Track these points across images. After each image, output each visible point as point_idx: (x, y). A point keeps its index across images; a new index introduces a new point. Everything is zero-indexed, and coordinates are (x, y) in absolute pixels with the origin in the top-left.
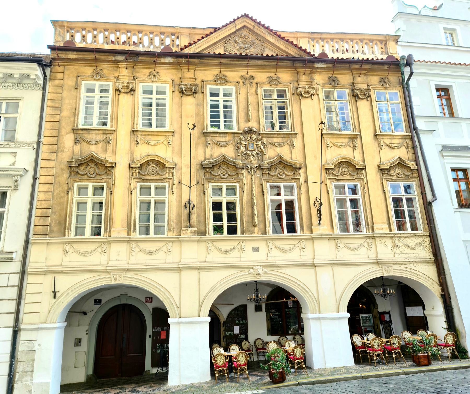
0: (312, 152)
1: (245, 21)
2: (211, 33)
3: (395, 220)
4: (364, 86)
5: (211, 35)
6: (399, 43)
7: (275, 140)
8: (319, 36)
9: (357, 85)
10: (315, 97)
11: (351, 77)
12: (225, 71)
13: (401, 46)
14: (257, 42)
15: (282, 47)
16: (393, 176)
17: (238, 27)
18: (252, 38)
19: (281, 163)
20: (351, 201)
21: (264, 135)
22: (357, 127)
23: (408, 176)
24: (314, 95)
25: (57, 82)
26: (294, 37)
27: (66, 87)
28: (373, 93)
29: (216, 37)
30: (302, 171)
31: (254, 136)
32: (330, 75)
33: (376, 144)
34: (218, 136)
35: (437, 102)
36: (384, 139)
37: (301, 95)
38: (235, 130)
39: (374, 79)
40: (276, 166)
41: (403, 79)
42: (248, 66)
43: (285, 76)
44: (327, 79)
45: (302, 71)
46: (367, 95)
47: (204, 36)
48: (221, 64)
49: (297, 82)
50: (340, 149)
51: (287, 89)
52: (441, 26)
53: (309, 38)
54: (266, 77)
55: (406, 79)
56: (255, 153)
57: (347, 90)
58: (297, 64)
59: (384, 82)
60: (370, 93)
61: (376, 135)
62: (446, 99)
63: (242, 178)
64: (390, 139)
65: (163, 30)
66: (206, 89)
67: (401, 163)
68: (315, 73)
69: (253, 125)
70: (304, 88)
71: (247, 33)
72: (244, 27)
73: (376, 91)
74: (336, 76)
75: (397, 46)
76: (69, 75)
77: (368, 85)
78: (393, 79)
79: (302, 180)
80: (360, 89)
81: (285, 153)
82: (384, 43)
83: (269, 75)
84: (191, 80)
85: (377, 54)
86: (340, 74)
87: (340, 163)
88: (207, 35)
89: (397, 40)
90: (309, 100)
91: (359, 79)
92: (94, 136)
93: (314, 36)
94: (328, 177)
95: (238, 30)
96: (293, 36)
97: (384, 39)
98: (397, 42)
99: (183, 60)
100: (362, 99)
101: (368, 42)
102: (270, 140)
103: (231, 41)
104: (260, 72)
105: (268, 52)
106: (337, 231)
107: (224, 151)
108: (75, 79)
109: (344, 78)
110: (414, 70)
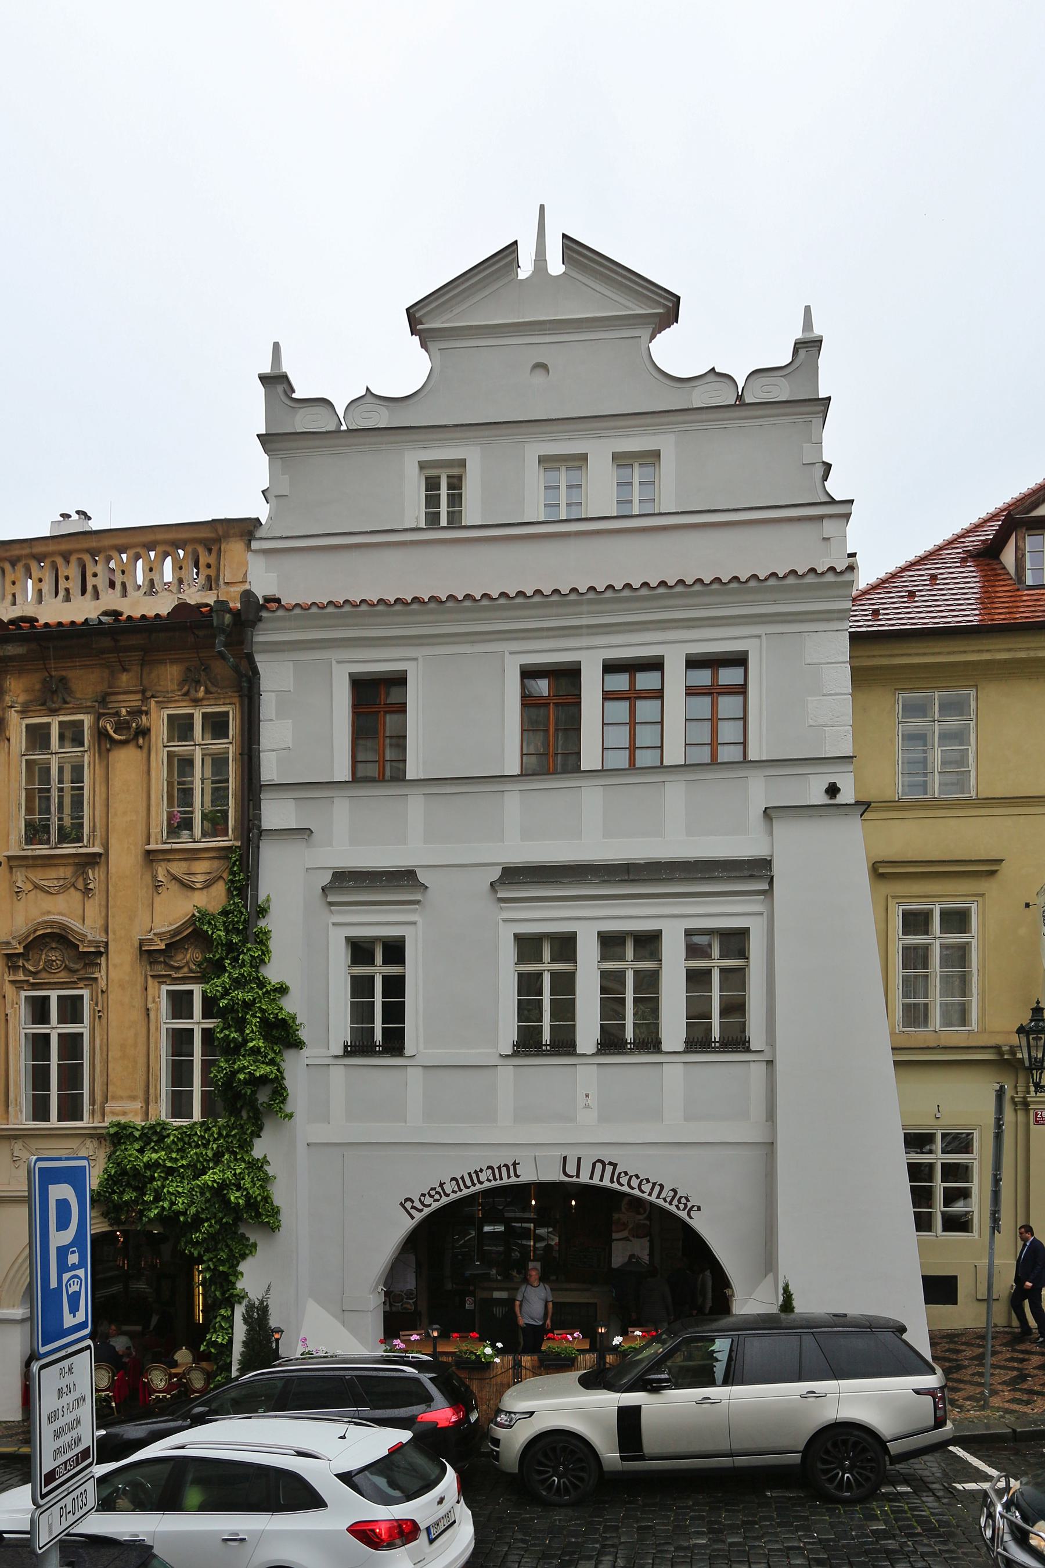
13: (265, 552)
33: (148, 878)
36: (169, 860)
50: (50, 897)
64: (185, 859)
75: (250, 556)
94: (12, 978)
98: (249, 545)
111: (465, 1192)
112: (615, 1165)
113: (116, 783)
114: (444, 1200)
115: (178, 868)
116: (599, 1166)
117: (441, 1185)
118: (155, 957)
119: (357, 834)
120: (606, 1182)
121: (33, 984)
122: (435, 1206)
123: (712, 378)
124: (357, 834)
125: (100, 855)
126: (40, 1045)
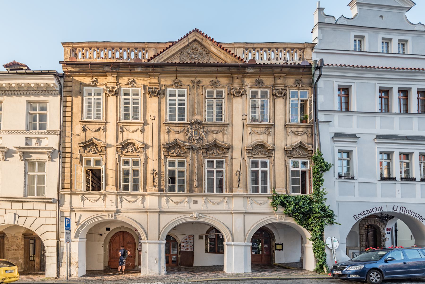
0: (239, 136)
1: (196, 35)
2: (170, 46)
3: (291, 185)
4: (281, 87)
5: (170, 48)
6: (314, 50)
7: (213, 129)
8: (252, 46)
9: (276, 86)
10: (244, 97)
11: (273, 79)
12: (180, 77)
14: (204, 53)
15: (222, 56)
16: (294, 155)
17: (190, 41)
18: (200, 50)
19: (215, 145)
20: (262, 172)
21: (206, 125)
22: (272, 119)
23: (305, 155)
24: (243, 95)
25: (68, 89)
26: (232, 48)
27: (74, 92)
28: (289, 92)
29: (174, 50)
30: (229, 151)
31: (198, 126)
32: (257, 78)
34: (174, 126)
35: (337, 99)
37: (234, 95)
38: (185, 121)
39: (291, 81)
40: (212, 147)
41: (313, 81)
42: (196, 73)
43: (223, 81)
44: (254, 81)
45: (236, 75)
46: (283, 94)
47: (165, 49)
48: (177, 72)
49: (232, 84)
51: (224, 90)
52: (352, 34)
53: (244, 48)
54: (209, 81)
55: (315, 81)
56: (198, 138)
57: (268, 90)
58: (233, 70)
59: (298, 83)
60: (285, 92)
61: (285, 125)
62: (345, 97)
63: (188, 155)
64: (296, 128)
65: (136, 45)
66: (166, 91)
67: (301, 146)
68: (245, 77)
69: (197, 118)
70: (236, 89)
71: (197, 46)
72: (195, 40)
73: (291, 90)
74: (261, 79)
76: (75, 83)
77: (285, 86)
78: (306, 80)
79: (229, 158)
80: (278, 89)
81: (220, 138)
82: (302, 51)
83: (211, 79)
84: (156, 84)
85: (295, 59)
86: (265, 77)
87: (257, 145)
88: (167, 48)
89: (313, 47)
90: (239, 99)
91: (279, 81)
92: (93, 126)
93: (248, 47)
95: (191, 43)
96: (231, 46)
97: (303, 47)
99: (150, 69)
100: (279, 97)
101: (290, 50)
102: (209, 129)
103: (185, 53)
104: (205, 77)
105: (212, 61)
106: (250, 192)
107: (177, 136)
108: (79, 86)
109: (268, 81)
110: (323, 73)
111: (370, 214)
112: (405, 208)
113: (277, 107)
114: (364, 216)
115: (294, 130)
116: (402, 208)
117: (364, 212)
118: (288, 152)
119: (340, 124)
120: (403, 212)
121: (254, 157)
122: (362, 217)
123: (419, 25)
124: (340, 124)
125: (272, 125)
126: (255, 173)
